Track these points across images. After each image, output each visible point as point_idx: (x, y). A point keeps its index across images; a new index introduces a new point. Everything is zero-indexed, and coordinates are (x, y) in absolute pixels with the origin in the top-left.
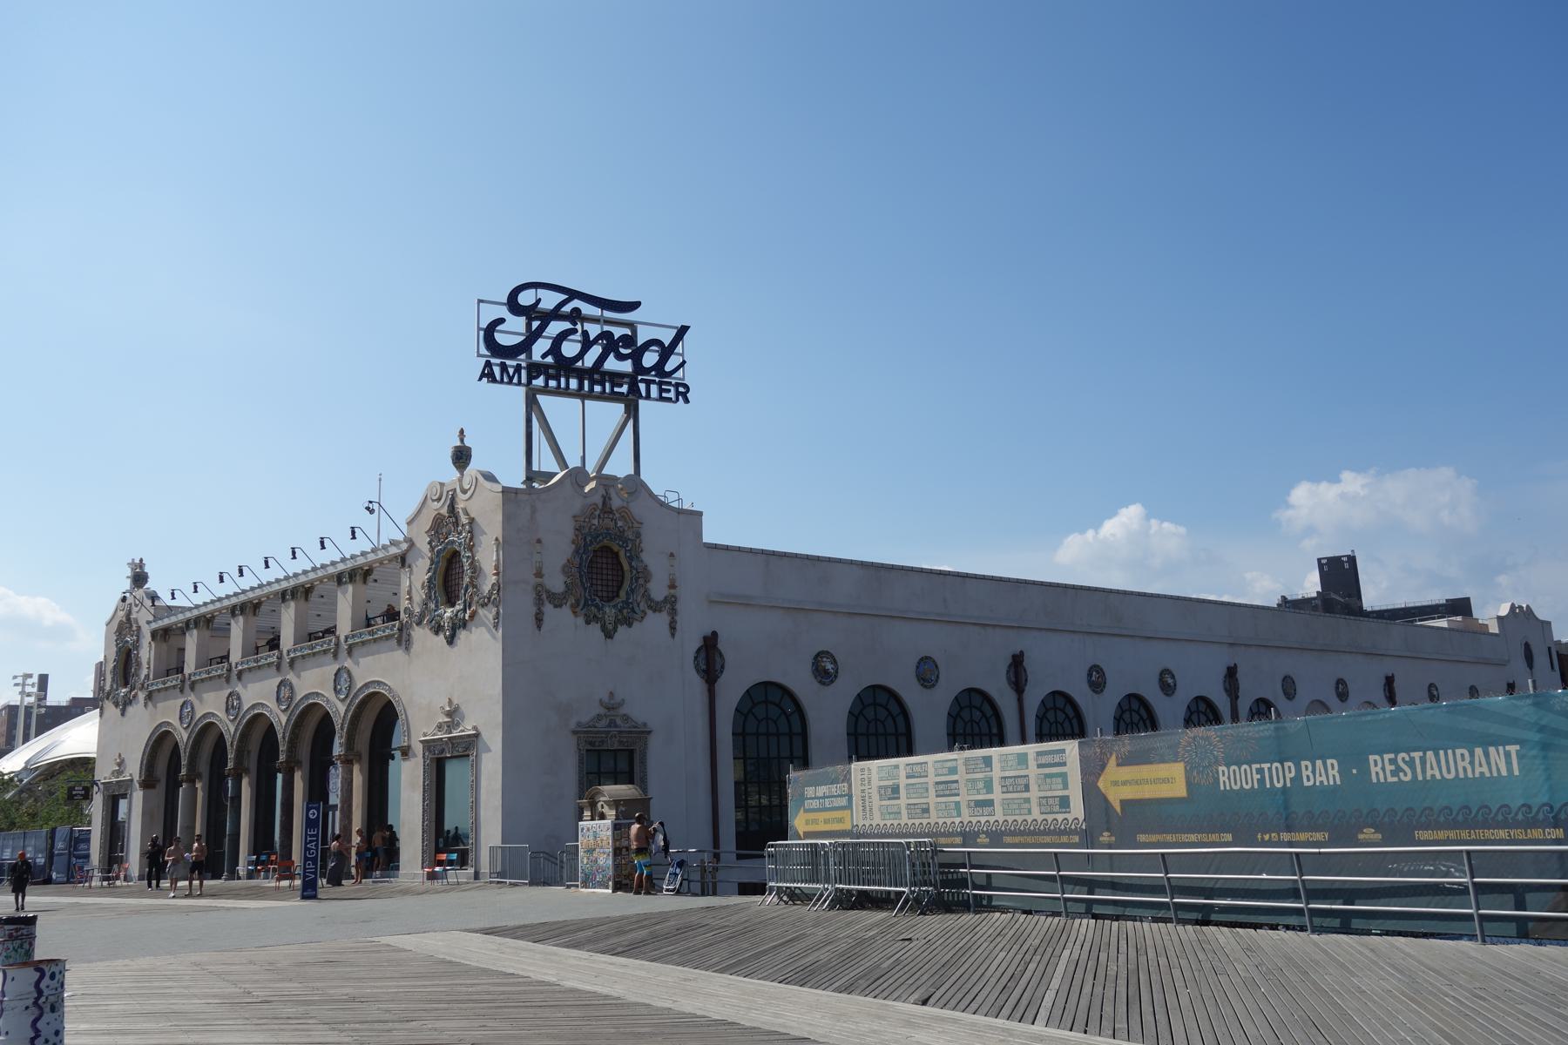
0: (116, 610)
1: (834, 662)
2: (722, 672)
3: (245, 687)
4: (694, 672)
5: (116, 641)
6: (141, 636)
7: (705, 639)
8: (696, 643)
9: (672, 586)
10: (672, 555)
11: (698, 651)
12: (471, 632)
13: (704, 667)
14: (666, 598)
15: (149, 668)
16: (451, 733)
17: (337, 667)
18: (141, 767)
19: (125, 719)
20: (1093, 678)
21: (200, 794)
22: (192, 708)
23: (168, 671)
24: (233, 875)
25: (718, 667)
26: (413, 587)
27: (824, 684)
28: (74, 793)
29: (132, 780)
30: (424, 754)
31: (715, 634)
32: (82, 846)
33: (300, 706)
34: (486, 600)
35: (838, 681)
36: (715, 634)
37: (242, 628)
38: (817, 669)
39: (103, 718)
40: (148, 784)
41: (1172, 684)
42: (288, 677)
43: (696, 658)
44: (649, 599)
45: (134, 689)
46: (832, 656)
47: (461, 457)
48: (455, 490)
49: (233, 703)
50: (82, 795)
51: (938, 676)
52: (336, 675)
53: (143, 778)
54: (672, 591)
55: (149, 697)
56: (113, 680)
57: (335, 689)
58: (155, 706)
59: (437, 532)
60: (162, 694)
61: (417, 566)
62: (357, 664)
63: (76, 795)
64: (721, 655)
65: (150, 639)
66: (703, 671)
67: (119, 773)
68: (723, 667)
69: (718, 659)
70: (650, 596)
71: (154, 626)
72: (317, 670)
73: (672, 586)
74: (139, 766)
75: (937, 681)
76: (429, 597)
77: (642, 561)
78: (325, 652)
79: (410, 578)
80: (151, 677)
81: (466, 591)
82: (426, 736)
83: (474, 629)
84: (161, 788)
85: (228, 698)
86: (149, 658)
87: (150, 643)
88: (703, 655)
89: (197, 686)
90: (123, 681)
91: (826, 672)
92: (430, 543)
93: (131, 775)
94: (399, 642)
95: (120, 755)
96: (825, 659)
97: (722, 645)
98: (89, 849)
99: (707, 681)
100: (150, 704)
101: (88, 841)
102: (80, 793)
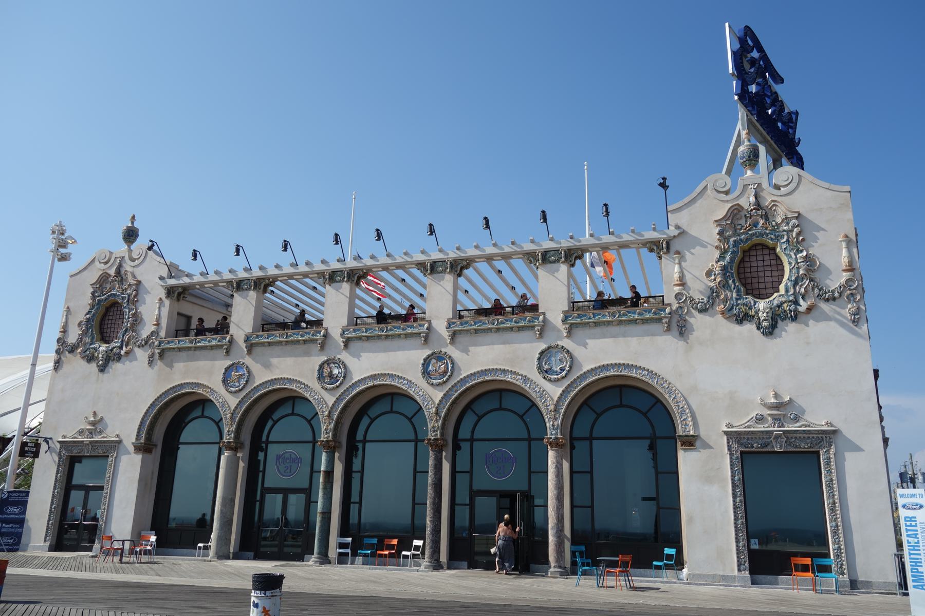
0: (93, 261)
3: (358, 357)
5: (93, 294)
6: (141, 291)
12: (807, 325)
15: (158, 325)
16: (783, 426)
17: (544, 346)
18: (139, 429)
19: (105, 376)
21: (242, 464)
22: (249, 371)
23: (177, 331)
24: (324, 559)
26: (685, 272)
28: (26, 449)
29: (120, 442)
30: (729, 447)
32: (12, 509)
33: (468, 382)
34: (143, 342)
37: (254, 303)
39: (61, 372)
40: (144, 448)
42: (444, 350)
45: (127, 346)
47: (131, 235)
48: (760, 185)
49: (331, 372)
50: (32, 452)
52: (541, 354)
53: (143, 441)
55: (162, 355)
56: (84, 333)
57: (540, 369)
58: (171, 366)
59: (732, 222)
60: (184, 354)
61: (693, 254)
62: (585, 345)
63: (27, 452)
65: (163, 295)
67: (91, 432)
71: (172, 282)
72: (501, 346)
74: (137, 427)
76: (725, 285)
78: (314, 341)
79: (680, 264)
80: (163, 334)
81: (796, 283)
82: (733, 427)
83: (811, 322)
84: (157, 452)
85: (321, 367)
86: (159, 315)
87: (161, 299)
89: (167, 354)
90: (100, 337)
92: (721, 233)
93: (118, 436)
94: (669, 329)
95: (95, 414)
98: (24, 513)
100: (159, 364)
101: (24, 504)
102: (32, 449)
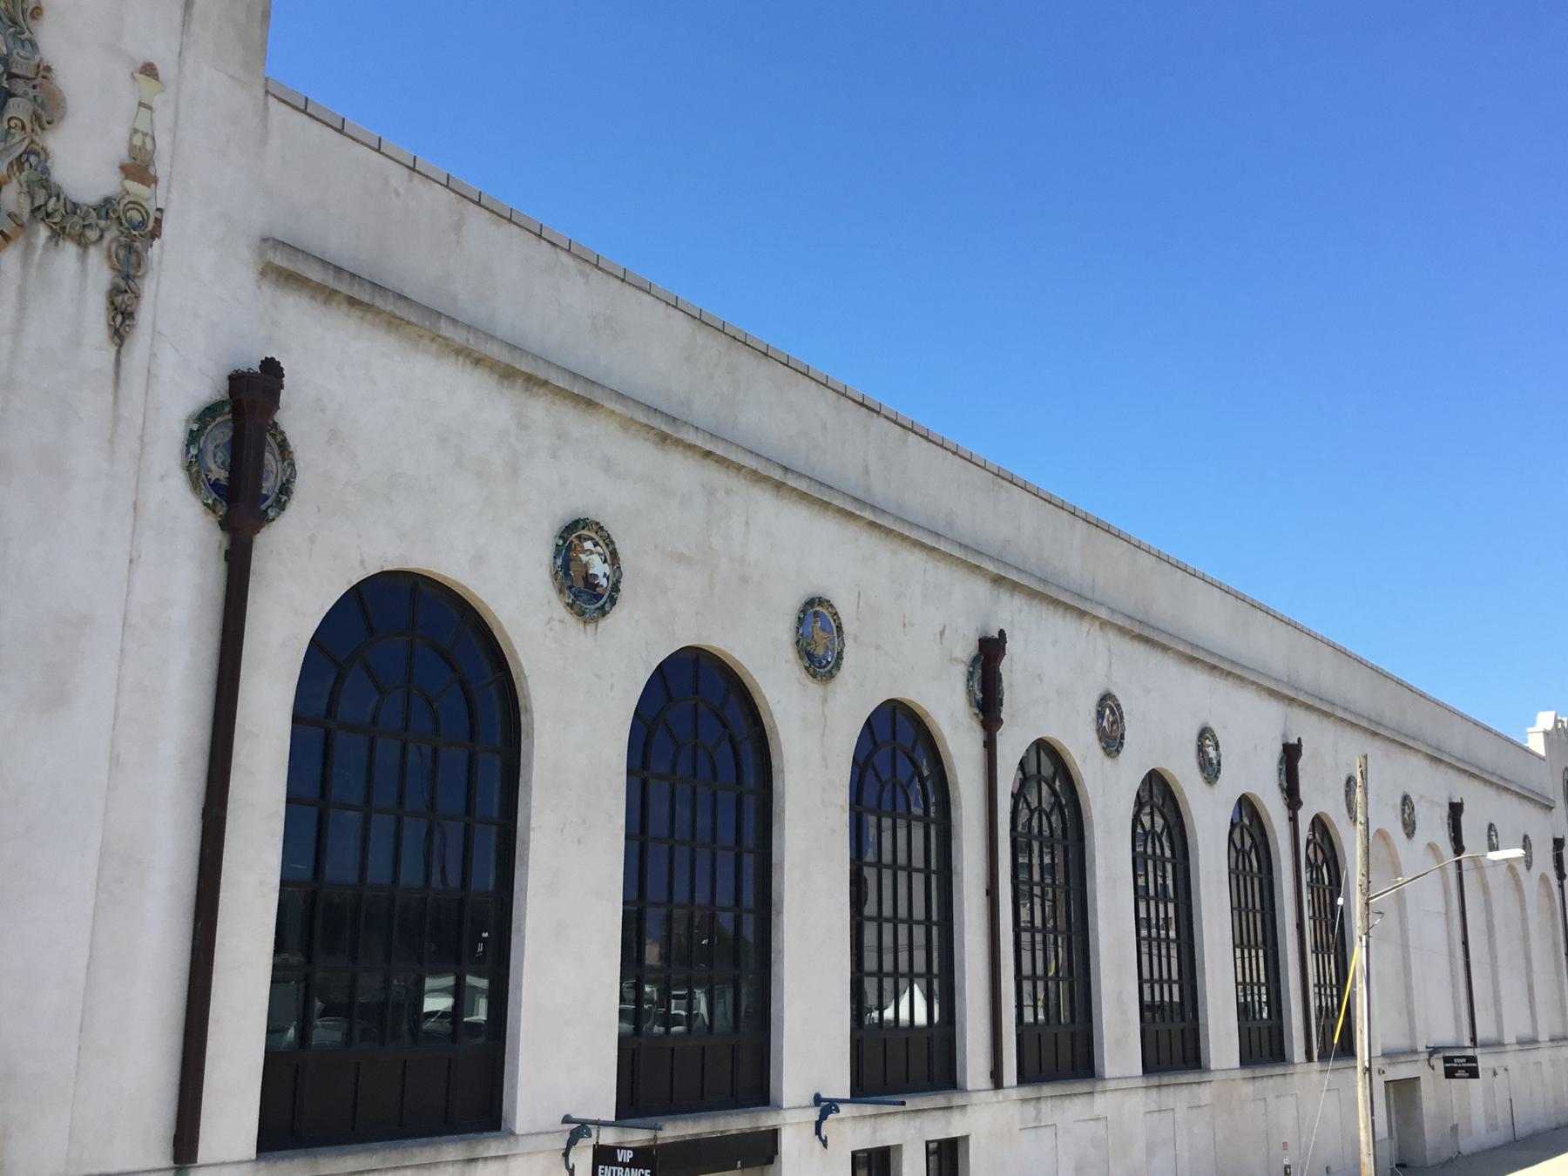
1: (613, 558)
2: (281, 506)
4: (178, 482)
7: (238, 381)
8: (205, 387)
9: (138, 168)
10: (149, 70)
11: (206, 415)
13: (219, 474)
14: (107, 201)
20: (1105, 724)
25: (269, 486)
27: (581, 614)
31: (272, 370)
35: (617, 616)
36: (272, 370)
38: (566, 567)
41: (1215, 762)
43: (193, 438)
44: (43, 182)
46: (609, 542)
51: (840, 657)
54: (136, 188)
64: (284, 448)
66: (215, 486)
68: (285, 489)
69: (271, 460)
70: (46, 171)
73: (138, 168)
75: (838, 665)
77: (34, 45)
88: (220, 434)
91: (589, 581)
96: (588, 545)
97: (293, 417)
99: (224, 525)
